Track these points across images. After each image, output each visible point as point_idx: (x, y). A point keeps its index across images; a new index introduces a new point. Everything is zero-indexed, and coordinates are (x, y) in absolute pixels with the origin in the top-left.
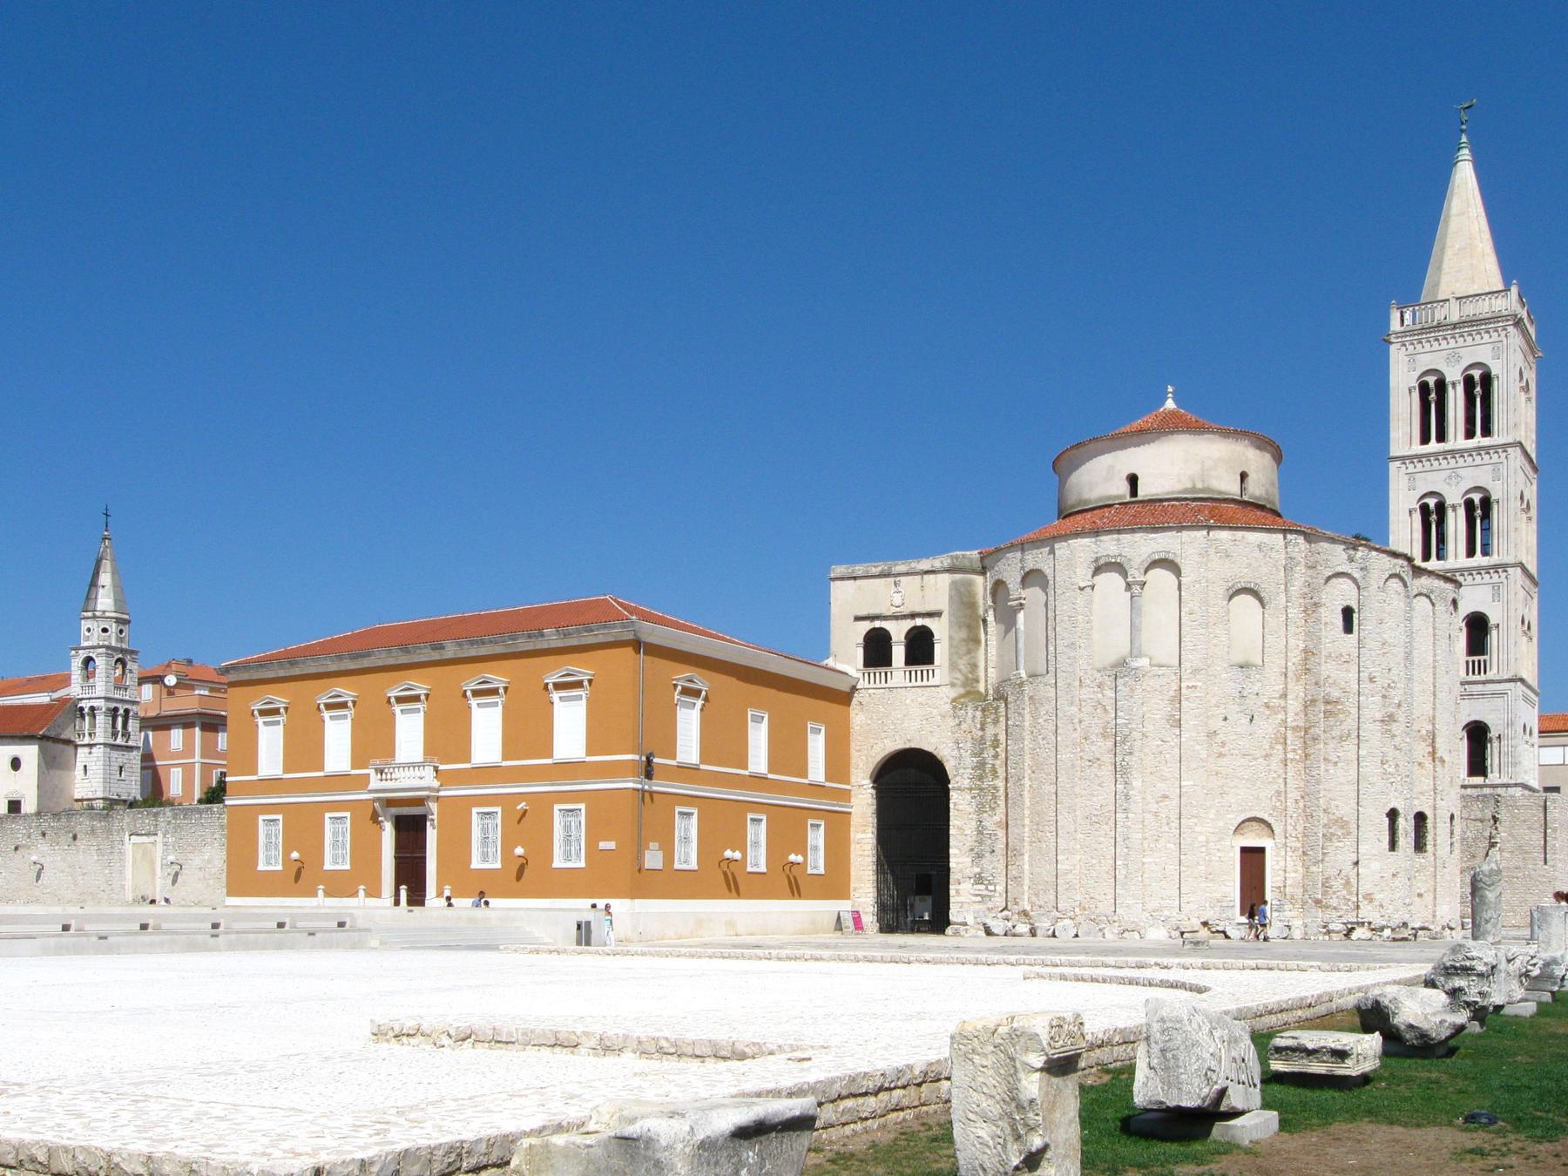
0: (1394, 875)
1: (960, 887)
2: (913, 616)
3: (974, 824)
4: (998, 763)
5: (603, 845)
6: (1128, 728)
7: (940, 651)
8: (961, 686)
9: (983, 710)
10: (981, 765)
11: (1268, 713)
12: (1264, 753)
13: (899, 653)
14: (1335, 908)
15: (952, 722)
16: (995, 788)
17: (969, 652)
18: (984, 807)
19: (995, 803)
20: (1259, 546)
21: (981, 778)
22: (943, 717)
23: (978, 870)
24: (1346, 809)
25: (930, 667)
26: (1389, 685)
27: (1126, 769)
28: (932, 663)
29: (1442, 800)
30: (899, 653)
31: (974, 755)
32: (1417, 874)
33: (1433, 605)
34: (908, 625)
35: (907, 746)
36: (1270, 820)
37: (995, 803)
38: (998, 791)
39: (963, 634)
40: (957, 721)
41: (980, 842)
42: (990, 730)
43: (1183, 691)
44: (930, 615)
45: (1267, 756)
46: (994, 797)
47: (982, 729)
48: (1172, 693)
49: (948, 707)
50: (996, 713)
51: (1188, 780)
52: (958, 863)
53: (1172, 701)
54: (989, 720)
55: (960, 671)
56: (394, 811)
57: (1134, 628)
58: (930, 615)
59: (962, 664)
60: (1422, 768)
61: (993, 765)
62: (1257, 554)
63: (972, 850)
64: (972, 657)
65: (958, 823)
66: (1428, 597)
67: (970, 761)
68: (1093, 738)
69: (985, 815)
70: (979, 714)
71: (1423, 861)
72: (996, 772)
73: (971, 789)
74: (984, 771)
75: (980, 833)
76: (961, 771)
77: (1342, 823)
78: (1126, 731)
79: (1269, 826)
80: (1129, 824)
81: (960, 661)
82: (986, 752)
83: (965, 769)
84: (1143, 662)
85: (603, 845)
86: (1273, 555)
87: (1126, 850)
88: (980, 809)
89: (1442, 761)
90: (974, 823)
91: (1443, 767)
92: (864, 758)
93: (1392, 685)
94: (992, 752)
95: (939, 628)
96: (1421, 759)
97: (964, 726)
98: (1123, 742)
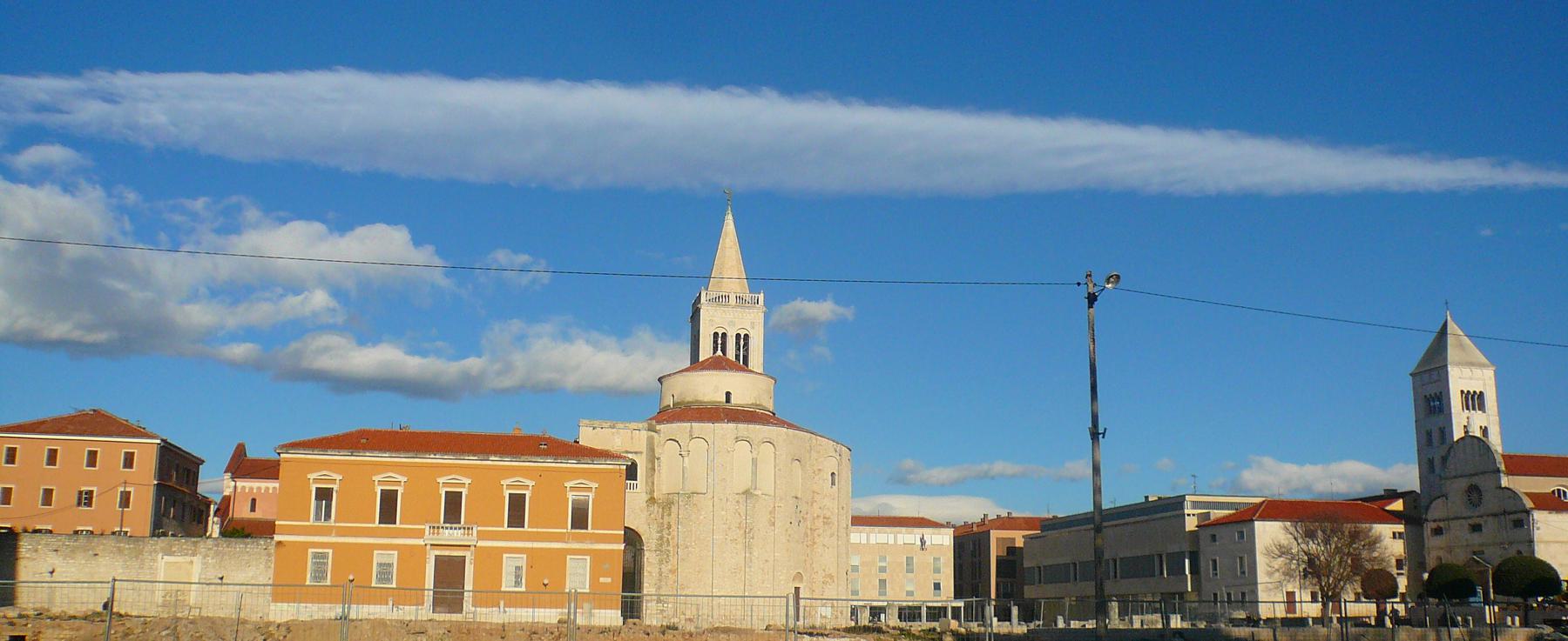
3: (657, 570)
4: (670, 537)
5: (602, 580)
7: (641, 472)
9: (663, 508)
10: (661, 538)
21: (661, 545)
22: (642, 511)
24: (833, 571)
31: (658, 532)
44: (636, 453)
46: (668, 556)
47: (662, 518)
48: (770, 509)
49: (645, 505)
53: (770, 513)
56: (438, 553)
57: (754, 473)
58: (636, 453)
59: (649, 480)
65: (649, 569)
73: (656, 551)
75: (661, 575)
77: (831, 577)
84: (758, 492)
85: (602, 580)
88: (661, 562)
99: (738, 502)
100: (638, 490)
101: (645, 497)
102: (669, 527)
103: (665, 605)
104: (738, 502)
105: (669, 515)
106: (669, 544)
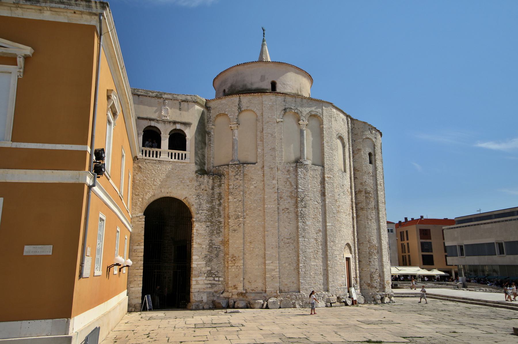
1: (200, 278)
2: (175, 123)
4: (221, 208)
6: (303, 194)
8: (199, 165)
9: (213, 179)
10: (212, 208)
13: (165, 143)
14: (376, 288)
15: (196, 184)
16: (220, 222)
17: (202, 148)
18: (213, 232)
19: (219, 230)
22: (191, 181)
23: (209, 268)
25: (184, 152)
27: (303, 215)
28: (185, 150)
30: (165, 143)
34: (171, 128)
35: (168, 195)
37: (219, 230)
38: (221, 224)
39: (200, 138)
40: (198, 183)
41: (211, 252)
42: (217, 190)
43: (326, 179)
45: (349, 214)
46: (219, 227)
47: (213, 189)
49: (194, 175)
50: (220, 182)
51: (329, 223)
52: (197, 265)
54: (216, 185)
55: (199, 156)
61: (218, 209)
63: (206, 257)
64: (203, 151)
67: (206, 206)
68: (285, 197)
69: (214, 237)
70: (211, 181)
72: (220, 213)
74: (213, 212)
76: (200, 211)
78: (303, 196)
80: (305, 244)
81: (199, 152)
82: (214, 202)
83: (203, 210)
87: (304, 258)
88: (211, 233)
90: (207, 241)
92: (140, 199)
94: (218, 202)
95: (190, 134)
97: (203, 187)
98: (302, 201)
99: (288, 171)
100: (187, 160)
101: (194, 168)
102: (220, 197)
103: (217, 279)
104: (288, 171)
105: (220, 186)
106: (220, 216)
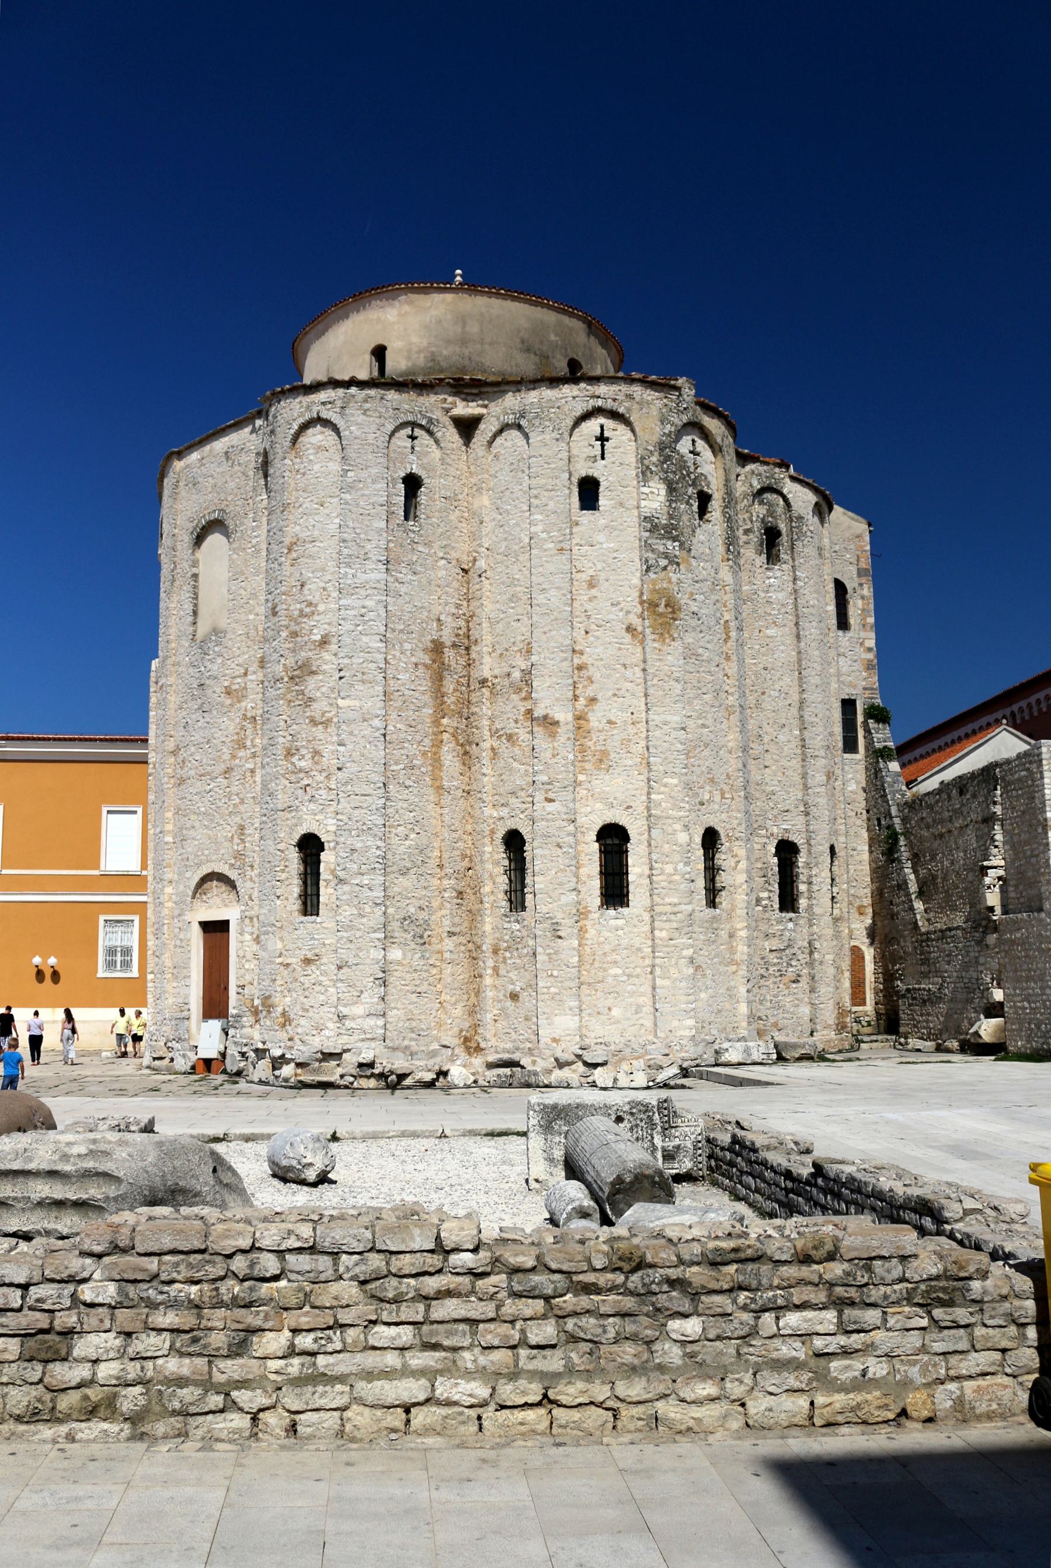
0: (307, 961)
11: (228, 702)
12: (223, 767)
20: (226, 453)
26: (301, 611)
29: (550, 800)
32: (508, 954)
33: (527, 437)
36: (233, 875)
45: (228, 771)
60: (514, 744)
62: (225, 467)
66: (519, 427)
71: (518, 927)
79: (231, 884)
86: (244, 458)
89: (549, 723)
91: (553, 735)
93: (308, 610)
96: (511, 727)
